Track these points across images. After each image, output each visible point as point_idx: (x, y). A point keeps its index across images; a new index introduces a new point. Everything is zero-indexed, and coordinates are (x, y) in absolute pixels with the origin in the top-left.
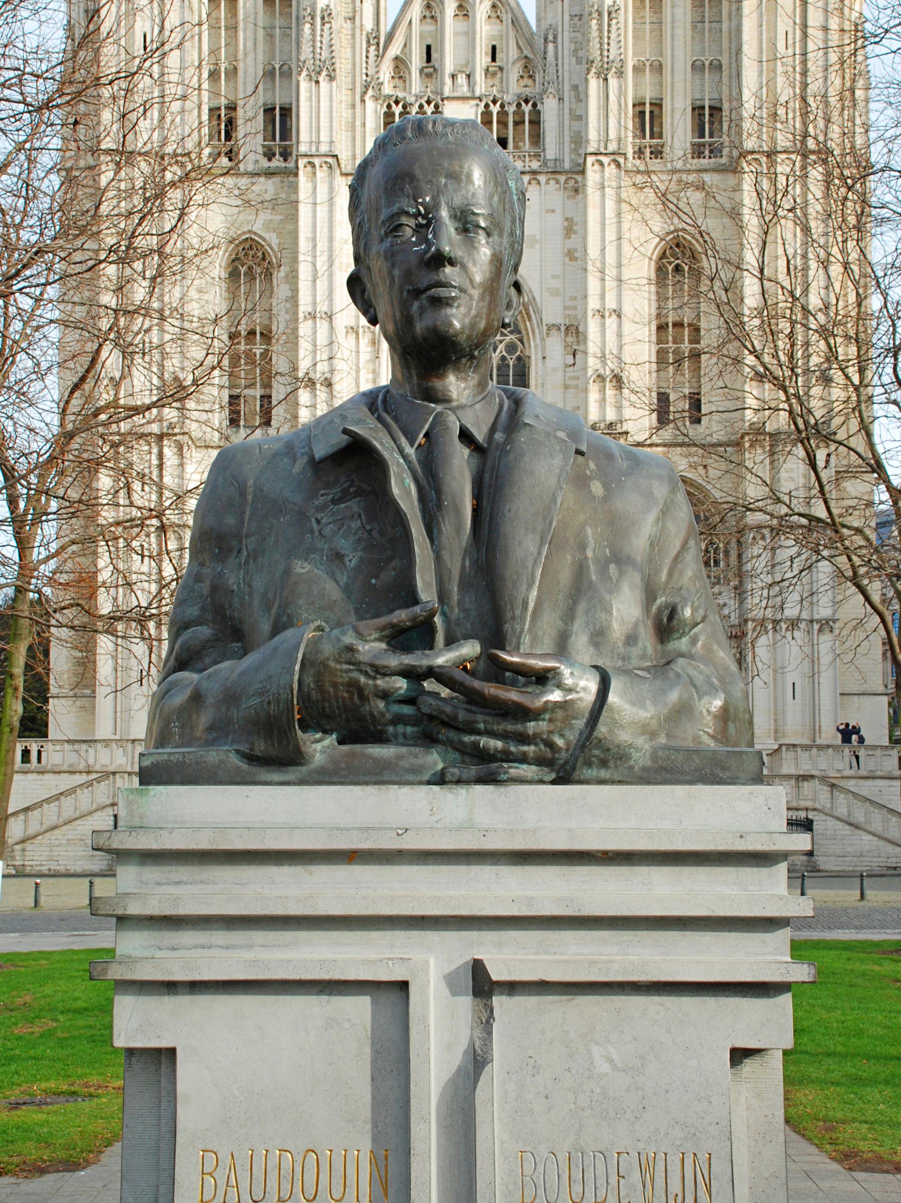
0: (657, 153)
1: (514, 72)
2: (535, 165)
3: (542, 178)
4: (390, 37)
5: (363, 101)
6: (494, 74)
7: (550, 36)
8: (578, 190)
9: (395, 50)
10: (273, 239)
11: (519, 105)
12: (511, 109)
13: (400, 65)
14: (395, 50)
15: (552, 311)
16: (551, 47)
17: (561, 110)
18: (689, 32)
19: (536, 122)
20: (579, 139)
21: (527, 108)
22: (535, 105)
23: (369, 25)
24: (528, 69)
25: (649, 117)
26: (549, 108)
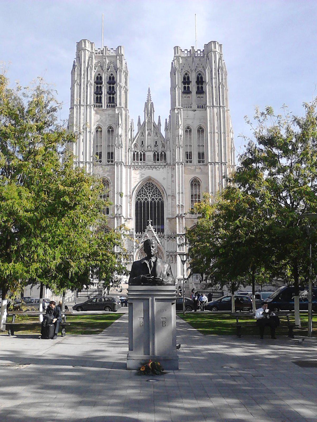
0: (191, 162)
1: (160, 146)
2: (165, 164)
3: (167, 167)
4: (134, 139)
5: (128, 152)
6: (156, 147)
7: (168, 140)
8: (174, 169)
9: (134, 142)
10: (109, 178)
11: (161, 153)
12: (160, 153)
13: (136, 146)
14: (134, 142)
15: (169, 192)
16: (168, 142)
17: (170, 154)
18: (197, 139)
19: (165, 155)
20: (174, 159)
21: (163, 153)
22: (165, 153)
23: (129, 137)
24: (163, 146)
25: (189, 156)
26: (168, 153)
